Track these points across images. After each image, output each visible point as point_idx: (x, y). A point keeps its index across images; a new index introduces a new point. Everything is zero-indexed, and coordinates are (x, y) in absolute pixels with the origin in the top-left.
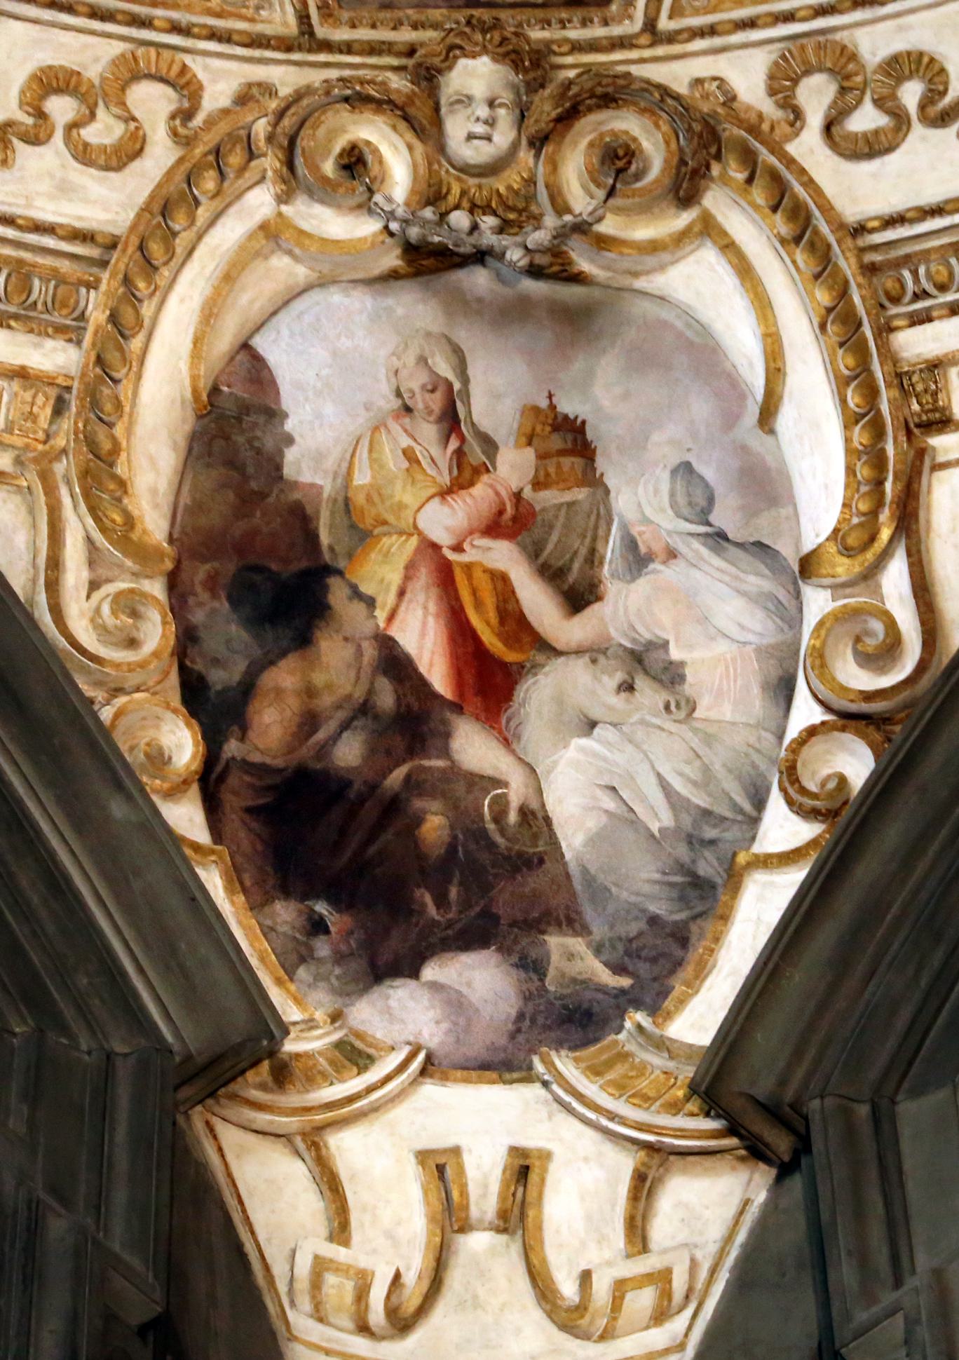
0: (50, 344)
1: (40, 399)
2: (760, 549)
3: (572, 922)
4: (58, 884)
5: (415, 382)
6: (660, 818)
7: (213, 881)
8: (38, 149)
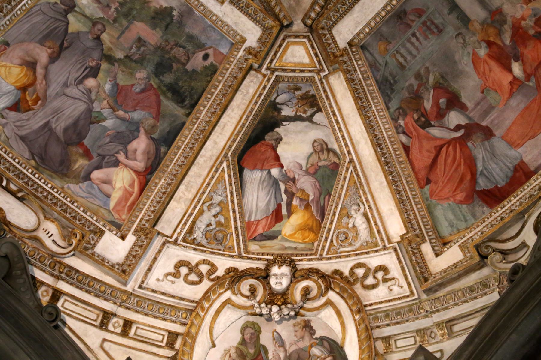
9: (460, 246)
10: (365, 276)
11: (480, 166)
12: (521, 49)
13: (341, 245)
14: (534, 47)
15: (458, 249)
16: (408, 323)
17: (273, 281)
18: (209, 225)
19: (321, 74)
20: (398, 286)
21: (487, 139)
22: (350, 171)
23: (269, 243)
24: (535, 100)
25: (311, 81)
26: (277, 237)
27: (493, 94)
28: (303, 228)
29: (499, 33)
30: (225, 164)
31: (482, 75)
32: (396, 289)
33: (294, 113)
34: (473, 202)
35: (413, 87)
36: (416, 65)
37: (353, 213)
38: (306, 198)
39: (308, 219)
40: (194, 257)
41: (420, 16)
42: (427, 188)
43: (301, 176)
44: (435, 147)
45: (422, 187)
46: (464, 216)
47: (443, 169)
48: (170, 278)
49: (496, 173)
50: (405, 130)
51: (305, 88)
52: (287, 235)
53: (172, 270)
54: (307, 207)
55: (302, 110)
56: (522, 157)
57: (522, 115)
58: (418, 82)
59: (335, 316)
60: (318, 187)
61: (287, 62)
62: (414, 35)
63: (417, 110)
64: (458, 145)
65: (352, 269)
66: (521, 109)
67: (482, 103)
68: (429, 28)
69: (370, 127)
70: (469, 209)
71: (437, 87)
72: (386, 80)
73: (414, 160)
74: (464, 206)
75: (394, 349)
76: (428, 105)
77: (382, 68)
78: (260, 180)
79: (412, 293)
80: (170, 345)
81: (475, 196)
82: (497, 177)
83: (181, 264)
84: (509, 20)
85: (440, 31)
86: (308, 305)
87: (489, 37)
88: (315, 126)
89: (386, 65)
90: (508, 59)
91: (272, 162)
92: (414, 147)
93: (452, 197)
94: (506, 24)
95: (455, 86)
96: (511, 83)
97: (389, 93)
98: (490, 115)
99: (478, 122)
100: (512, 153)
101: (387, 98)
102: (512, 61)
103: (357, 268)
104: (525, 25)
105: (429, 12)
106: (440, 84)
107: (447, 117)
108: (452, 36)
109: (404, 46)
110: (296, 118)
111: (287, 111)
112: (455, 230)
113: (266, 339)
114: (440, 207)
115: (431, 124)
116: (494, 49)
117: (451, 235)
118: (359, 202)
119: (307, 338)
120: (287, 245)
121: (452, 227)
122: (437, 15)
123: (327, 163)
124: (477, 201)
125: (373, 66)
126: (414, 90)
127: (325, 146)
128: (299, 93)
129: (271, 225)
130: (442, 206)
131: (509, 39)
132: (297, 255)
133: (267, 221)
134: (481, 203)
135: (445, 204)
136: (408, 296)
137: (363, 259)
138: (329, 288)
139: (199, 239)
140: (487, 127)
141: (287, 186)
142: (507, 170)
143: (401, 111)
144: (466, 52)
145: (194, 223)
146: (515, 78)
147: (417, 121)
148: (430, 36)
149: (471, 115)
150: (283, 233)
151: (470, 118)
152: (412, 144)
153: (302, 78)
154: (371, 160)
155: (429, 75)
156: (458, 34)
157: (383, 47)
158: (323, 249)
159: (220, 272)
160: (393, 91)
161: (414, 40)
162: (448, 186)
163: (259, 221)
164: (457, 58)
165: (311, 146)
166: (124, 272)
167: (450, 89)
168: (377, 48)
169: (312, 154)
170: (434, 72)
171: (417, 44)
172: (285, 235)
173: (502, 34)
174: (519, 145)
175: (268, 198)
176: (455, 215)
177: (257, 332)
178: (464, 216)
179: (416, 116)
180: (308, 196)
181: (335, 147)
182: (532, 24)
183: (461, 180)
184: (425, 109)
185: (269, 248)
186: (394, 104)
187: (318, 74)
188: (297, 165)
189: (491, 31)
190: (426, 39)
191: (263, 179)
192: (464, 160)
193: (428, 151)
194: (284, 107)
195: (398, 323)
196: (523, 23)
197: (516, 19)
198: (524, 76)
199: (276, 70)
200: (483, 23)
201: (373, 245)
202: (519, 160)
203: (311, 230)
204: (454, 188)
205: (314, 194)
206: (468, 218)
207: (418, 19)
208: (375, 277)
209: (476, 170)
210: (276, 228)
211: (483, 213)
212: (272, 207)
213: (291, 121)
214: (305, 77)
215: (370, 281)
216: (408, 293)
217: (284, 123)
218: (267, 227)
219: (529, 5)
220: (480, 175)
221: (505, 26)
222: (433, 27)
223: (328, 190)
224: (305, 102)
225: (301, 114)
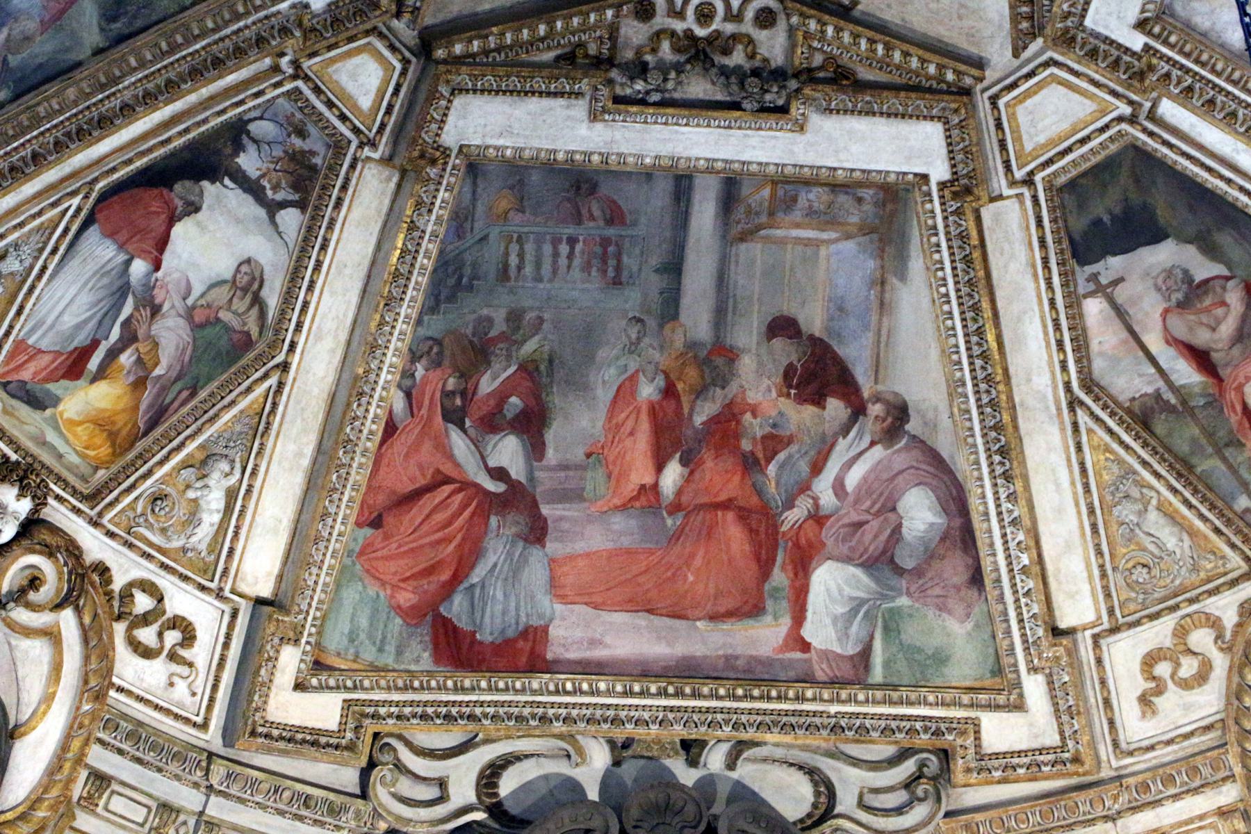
0: (1224, 789)
1: (1236, 822)
8: (1166, 695)
9: (348, 704)
13: (146, 520)
14: (726, 472)
15: (340, 704)
16: (158, 775)
19: (366, 149)
20: (190, 686)
21: (526, 540)
22: (266, 385)
23: (24, 410)
24: (651, 552)
25: (338, 147)
26: (44, 408)
27: (600, 474)
28: (102, 423)
29: (700, 392)
30: (76, 201)
31: (613, 428)
32: (181, 688)
33: (258, 173)
34: (417, 625)
35: (491, 327)
36: (528, 296)
37: (216, 475)
38: (150, 363)
39: (124, 410)
41: (610, 222)
42: (368, 531)
43: (173, 312)
44: (438, 471)
45: (359, 524)
46: (384, 638)
47: (417, 523)
49: (492, 612)
50: (414, 392)
51: (315, 143)
52: (66, 415)
54: (139, 384)
55: (274, 181)
56: (551, 620)
57: (612, 555)
58: (505, 328)
59: (45, 668)
60: (187, 359)
61: (335, 77)
62: (572, 241)
63: (462, 376)
64: (474, 504)
65: (131, 585)
66: (618, 545)
67: (571, 473)
68: (604, 259)
70: (400, 634)
71: (528, 369)
72: (459, 270)
73: (385, 461)
74: (398, 621)
75: (99, 810)
76: (487, 384)
77: (470, 240)
78: (103, 267)
79: (204, 726)
81: (429, 618)
82: (487, 620)
84: (733, 388)
85: (617, 282)
87: (679, 379)
88: (270, 230)
89: (481, 239)
90: (676, 445)
91: (148, 245)
92: (403, 437)
93: (393, 586)
94: (723, 388)
95: (556, 399)
96: (643, 487)
97: (442, 297)
98: (568, 506)
99: (538, 498)
100: (545, 603)
101: (432, 303)
102: (678, 455)
103: (144, 591)
104: (746, 424)
105: (629, 232)
106: (537, 369)
107: (498, 437)
108: (626, 311)
109: (539, 243)
110: (252, 188)
111: (249, 162)
112: (352, 651)
114: (360, 588)
115: (464, 423)
116: (670, 406)
117: (339, 654)
118: (238, 460)
120: (51, 437)
121: (352, 641)
122: (637, 251)
123: (235, 323)
124: (425, 631)
125: (460, 220)
126: (486, 334)
127: (256, 286)
128: (297, 142)
129: (52, 378)
130: (365, 587)
131: (705, 418)
132: (59, 479)
133: (53, 362)
134: (427, 638)
136: (195, 725)
137: (165, 582)
140: (545, 520)
141: (136, 314)
142: (513, 621)
143: (435, 350)
144: (622, 362)
146: (656, 486)
147: (447, 395)
148: (594, 272)
149: (539, 474)
150: (61, 407)
151: (531, 478)
152: (405, 427)
153: (328, 125)
154: (316, 391)
155: (533, 335)
156: (639, 320)
157: (504, 204)
158: (111, 505)
160: (451, 298)
161: (564, 249)
162: (402, 562)
163: (40, 351)
164: (602, 354)
165: (236, 265)
167: (544, 395)
168: (496, 198)
169: (224, 282)
170: (545, 339)
171: (563, 261)
172: (61, 414)
173: (702, 397)
174: (563, 599)
175: (88, 314)
176: (371, 625)
178: (384, 638)
179: (451, 383)
180: (156, 364)
181: (272, 300)
182: (759, 434)
183: (429, 571)
184: (476, 388)
185: (16, 422)
186: (436, 325)
187: (361, 146)
188: (184, 284)
189: (692, 373)
190: (583, 270)
191: (109, 267)
192: (463, 539)
193: (421, 467)
194: (251, 149)
195: (139, 761)
196: (748, 416)
197: (744, 399)
198: (671, 497)
199: (307, 78)
200: (692, 345)
201: (201, 564)
202: (542, 622)
203: (112, 436)
204: (408, 574)
205: (170, 368)
206: (387, 648)
207: (602, 223)
208: (160, 635)
209: (467, 576)
211: (417, 661)
212: (81, 339)
213: (241, 187)
214: (335, 128)
215: (147, 635)
216: (199, 720)
217: (227, 181)
218: (44, 374)
219: (782, 399)
220: (466, 589)
221: (718, 390)
222: (612, 262)
223: (197, 379)
224: (292, 167)
225: (268, 186)
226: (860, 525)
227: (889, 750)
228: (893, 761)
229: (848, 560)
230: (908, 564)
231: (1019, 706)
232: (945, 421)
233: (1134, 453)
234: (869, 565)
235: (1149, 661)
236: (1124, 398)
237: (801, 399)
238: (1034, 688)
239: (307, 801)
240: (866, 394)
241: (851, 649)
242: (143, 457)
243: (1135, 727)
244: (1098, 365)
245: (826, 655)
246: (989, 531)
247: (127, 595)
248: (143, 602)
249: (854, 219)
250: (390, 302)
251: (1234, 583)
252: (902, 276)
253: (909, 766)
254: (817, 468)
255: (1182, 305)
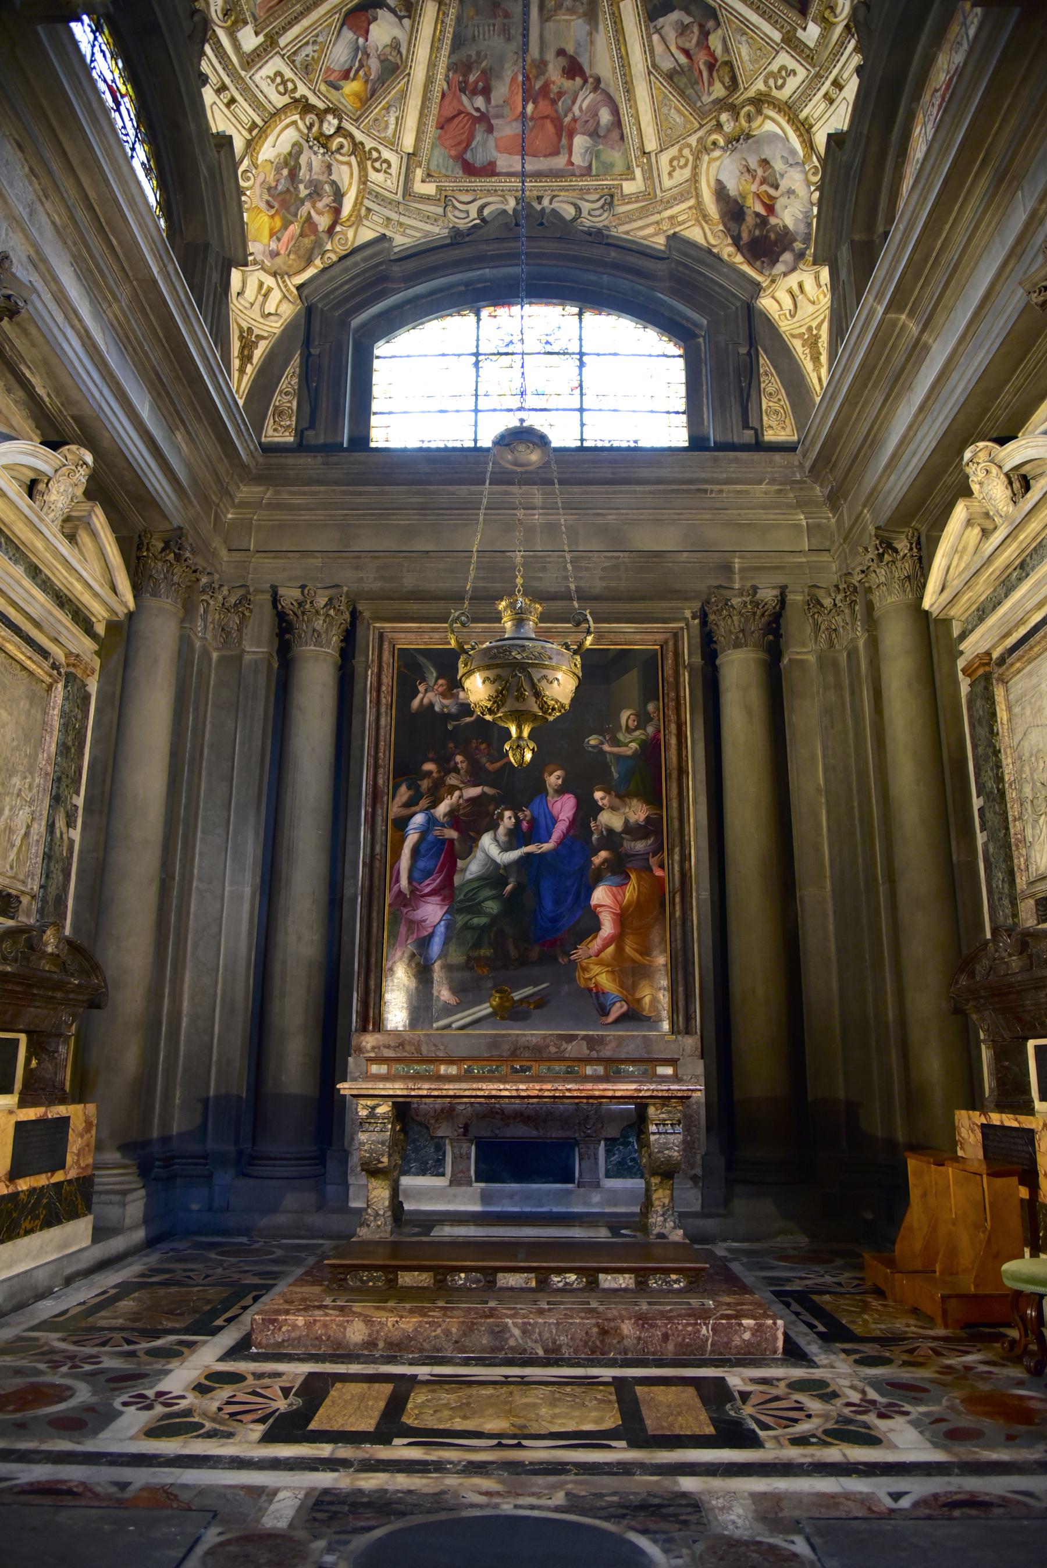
2: (797, 163)
3: (795, 240)
4: (721, 286)
5: (741, 168)
6: (800, 216)
7: (746, 268)
10: (376, 160)
11: (473, 145)
12: (540, 99)
17: (325, 125)
18: (307, 56)
23: (332, 90)
28: (356, 95)
29: (537, 77)
30: (337, 16)
32: (389, 181)
40: (288, 74)
48: (269, 80)
53: (272, 75)
54: (366, 82)
59: (348, 175)
68: (504, 31)
69: (432, 65)
71: (484, 72)
76: (472, 78)
80: (250, 131)
83: (278, 74)
84: (547, 75)
86: (338, 156)
91: (363, 32)
95: (493, 83)
100: (495, 153)
110: (393, 11)
113: (303, 160)
119: (326, 175)
120: (342, 100)
123: (393, 60)
125: (459, 19)
135: (443, 150)
137: (381, 148)
138: (353, 153)
139: (297, 63)
145: (300, 47)
147: (460, 83)
159: (297, 95)
160: (459, 48)
166: (248, 63)
174: (499, 151)
177: (300, 152)
181: (404, 52)
183: (459, 144)
186: (454, 59)
189: (534, 71)
200: (533, 61)
203: (360, 100)
210: (342, 83)
212: (347, 66)
215: (377, 165)
226: (587, 121)
227: (597, 196)
228: (598, 200)
229: (584, 134)
230: (602, 134)
231: (634, 179)
232: (612, 83)
233: (667, 89)
234: (590, 135)
235: (671, 161)
236: (665, 70)
237: (568, 78)
238: (638, 172)
239: (428, 217)
240: (587, 75)
241: (586, 164)
242: (370, 107)
243: (667, 183)
244: (657, 58)
245: (579, 167)
246: (625, 120)
247: (370, 152)
248: (375, 155)
249: (581, 11)
250: (439, 49)
251: (695, 132)
252: (597, 30)
253: (602, 201)
254: (574, 102)
255: (682, 34)
